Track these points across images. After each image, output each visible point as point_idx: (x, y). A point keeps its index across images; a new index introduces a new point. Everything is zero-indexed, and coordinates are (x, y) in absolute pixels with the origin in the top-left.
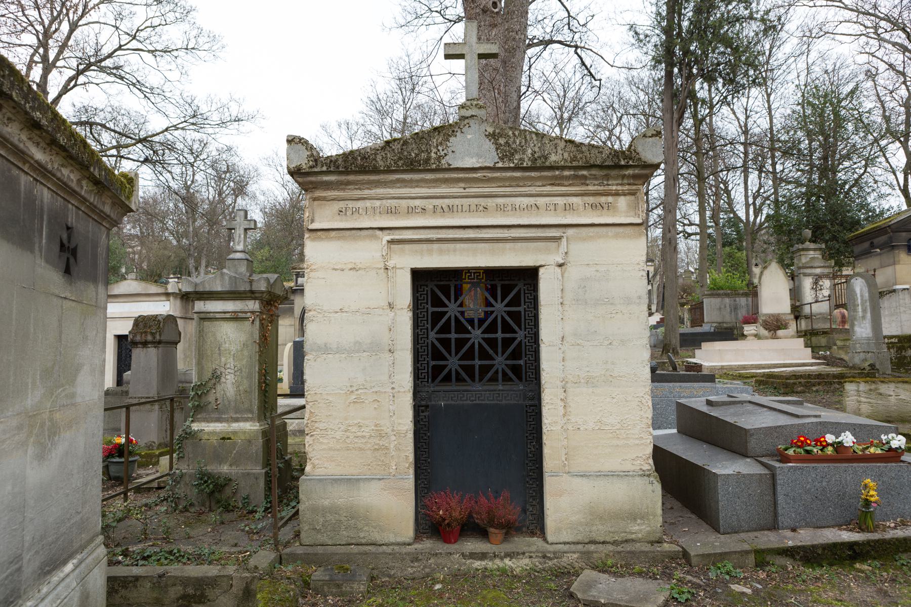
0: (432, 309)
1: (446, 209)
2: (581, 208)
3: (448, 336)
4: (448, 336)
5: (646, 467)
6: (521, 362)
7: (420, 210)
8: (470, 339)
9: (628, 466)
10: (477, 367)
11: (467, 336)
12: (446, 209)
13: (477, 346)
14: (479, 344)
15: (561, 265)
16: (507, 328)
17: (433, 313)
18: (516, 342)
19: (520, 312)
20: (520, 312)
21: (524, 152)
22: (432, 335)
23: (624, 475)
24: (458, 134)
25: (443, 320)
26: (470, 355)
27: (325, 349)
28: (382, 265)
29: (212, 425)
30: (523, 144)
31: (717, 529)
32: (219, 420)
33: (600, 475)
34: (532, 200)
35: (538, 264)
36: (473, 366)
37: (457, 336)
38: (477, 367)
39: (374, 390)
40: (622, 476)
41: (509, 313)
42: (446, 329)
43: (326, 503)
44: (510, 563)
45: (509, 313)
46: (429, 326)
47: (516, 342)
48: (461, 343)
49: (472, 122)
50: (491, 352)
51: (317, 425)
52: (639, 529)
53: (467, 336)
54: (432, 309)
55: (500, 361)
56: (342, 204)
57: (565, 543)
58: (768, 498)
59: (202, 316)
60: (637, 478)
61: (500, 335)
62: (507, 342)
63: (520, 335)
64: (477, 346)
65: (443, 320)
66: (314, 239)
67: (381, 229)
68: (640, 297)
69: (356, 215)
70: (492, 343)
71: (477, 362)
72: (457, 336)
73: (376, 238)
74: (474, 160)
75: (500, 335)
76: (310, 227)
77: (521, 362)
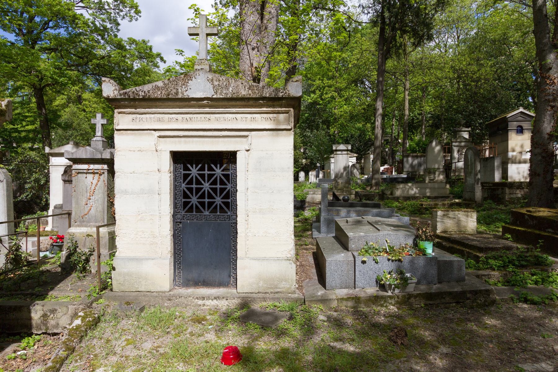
0: (183, 172)
1: (189, 119)
2: (260, 120)
3: (191, 186)
4: (191, 186)
5: (289, 256)
6: (229, 200)
7: (175, 120)
8: (203, 188)
9: (279, 255)
10: (206, 203)
11: (201, 186)
12: (189, 119)
13: (206, 192)
14: (208, 190)
15: (248, 151)
16: (222, 183)
17: (184, 174)
18: (227, 190)
19: (229, 174)
20: (229, 174)
21: (228, 89)
22: (184, 185)
23: (278, 259)
24: (193, 79)
25: (189, 178)
26: (203, 196)
27: (126, 192)
28: (155, 149)
29: (82, 228)
30: (227, 85)
31: (325, 289)
32: (86, 226)
33: (264, 259)
34: (234, 116)
35: (236, 150)
36: (205, 202)
37: (196, 186)
38: (206, 203)
39: (150, 214)
40: (276, 260)
41: (223, 175)
42: (190, 182)
43: (125, 270)
44: (217, 302)
45: (223, 175)
46: (182, 181)
47: (227, 190)
48: (198, 190)
49: (201, 73)
50: (214, 195)
51: (121, 231)
52: (283, 286)
53: (201, 186)
54: (183, 172)
55: (218, 200)
56: (134, 116)
57: (246, 293)
58: (351, 272)
59: (77, 171)
60: (284, 261)
61: (218, 186)
62: (222, 190)
63: (229, 187)
64: (206, 192)
65: (189, 178)
66: (119, 134)
67: (155, 130)
68: (289, 168)
69: (141, 122)
70: (215, 190)
71: (207, 200)
72: (196, 186)
73: (152, 134)
74: (202, 94)
75: (218, 186)
76: (117, 128)
77: (229, 200)
